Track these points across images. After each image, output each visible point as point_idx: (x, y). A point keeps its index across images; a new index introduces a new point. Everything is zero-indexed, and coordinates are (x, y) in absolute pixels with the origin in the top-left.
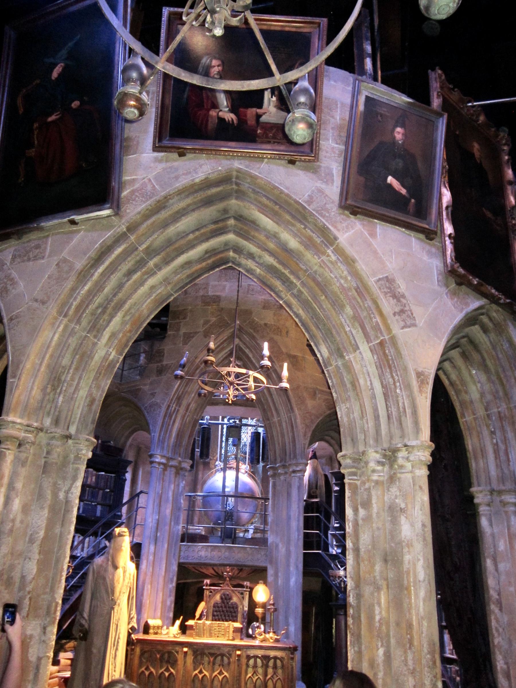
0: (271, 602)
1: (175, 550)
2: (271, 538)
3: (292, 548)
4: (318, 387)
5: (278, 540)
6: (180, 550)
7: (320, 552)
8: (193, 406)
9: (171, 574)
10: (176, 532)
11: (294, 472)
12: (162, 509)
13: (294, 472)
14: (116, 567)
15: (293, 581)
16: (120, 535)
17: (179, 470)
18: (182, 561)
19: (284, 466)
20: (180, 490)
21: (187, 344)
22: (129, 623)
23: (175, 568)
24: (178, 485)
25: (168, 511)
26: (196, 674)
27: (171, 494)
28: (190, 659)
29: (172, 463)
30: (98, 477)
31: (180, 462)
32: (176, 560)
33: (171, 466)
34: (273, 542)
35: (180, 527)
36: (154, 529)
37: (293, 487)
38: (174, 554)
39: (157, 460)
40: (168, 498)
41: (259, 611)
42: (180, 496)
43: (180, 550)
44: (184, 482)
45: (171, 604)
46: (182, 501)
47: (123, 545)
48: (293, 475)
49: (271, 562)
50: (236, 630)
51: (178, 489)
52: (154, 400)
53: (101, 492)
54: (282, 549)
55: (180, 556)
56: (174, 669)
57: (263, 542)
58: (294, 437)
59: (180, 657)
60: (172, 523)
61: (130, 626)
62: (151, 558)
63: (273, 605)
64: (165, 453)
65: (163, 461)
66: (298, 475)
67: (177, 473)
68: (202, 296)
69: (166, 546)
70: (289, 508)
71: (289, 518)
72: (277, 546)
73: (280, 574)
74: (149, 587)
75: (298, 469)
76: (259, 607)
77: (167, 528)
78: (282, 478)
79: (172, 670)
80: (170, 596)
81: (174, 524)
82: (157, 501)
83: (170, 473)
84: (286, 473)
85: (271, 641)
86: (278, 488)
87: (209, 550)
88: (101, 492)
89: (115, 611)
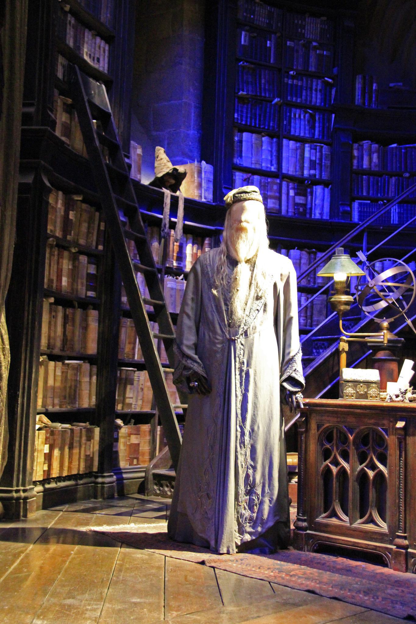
14: (234, 263)
16: (237, 200)
47: (243, 218)
53: (393, 180)
56: (385, 465)
59: (391, 440)
79: (381, 467)
88: (393, 180)
89: (238, 346)
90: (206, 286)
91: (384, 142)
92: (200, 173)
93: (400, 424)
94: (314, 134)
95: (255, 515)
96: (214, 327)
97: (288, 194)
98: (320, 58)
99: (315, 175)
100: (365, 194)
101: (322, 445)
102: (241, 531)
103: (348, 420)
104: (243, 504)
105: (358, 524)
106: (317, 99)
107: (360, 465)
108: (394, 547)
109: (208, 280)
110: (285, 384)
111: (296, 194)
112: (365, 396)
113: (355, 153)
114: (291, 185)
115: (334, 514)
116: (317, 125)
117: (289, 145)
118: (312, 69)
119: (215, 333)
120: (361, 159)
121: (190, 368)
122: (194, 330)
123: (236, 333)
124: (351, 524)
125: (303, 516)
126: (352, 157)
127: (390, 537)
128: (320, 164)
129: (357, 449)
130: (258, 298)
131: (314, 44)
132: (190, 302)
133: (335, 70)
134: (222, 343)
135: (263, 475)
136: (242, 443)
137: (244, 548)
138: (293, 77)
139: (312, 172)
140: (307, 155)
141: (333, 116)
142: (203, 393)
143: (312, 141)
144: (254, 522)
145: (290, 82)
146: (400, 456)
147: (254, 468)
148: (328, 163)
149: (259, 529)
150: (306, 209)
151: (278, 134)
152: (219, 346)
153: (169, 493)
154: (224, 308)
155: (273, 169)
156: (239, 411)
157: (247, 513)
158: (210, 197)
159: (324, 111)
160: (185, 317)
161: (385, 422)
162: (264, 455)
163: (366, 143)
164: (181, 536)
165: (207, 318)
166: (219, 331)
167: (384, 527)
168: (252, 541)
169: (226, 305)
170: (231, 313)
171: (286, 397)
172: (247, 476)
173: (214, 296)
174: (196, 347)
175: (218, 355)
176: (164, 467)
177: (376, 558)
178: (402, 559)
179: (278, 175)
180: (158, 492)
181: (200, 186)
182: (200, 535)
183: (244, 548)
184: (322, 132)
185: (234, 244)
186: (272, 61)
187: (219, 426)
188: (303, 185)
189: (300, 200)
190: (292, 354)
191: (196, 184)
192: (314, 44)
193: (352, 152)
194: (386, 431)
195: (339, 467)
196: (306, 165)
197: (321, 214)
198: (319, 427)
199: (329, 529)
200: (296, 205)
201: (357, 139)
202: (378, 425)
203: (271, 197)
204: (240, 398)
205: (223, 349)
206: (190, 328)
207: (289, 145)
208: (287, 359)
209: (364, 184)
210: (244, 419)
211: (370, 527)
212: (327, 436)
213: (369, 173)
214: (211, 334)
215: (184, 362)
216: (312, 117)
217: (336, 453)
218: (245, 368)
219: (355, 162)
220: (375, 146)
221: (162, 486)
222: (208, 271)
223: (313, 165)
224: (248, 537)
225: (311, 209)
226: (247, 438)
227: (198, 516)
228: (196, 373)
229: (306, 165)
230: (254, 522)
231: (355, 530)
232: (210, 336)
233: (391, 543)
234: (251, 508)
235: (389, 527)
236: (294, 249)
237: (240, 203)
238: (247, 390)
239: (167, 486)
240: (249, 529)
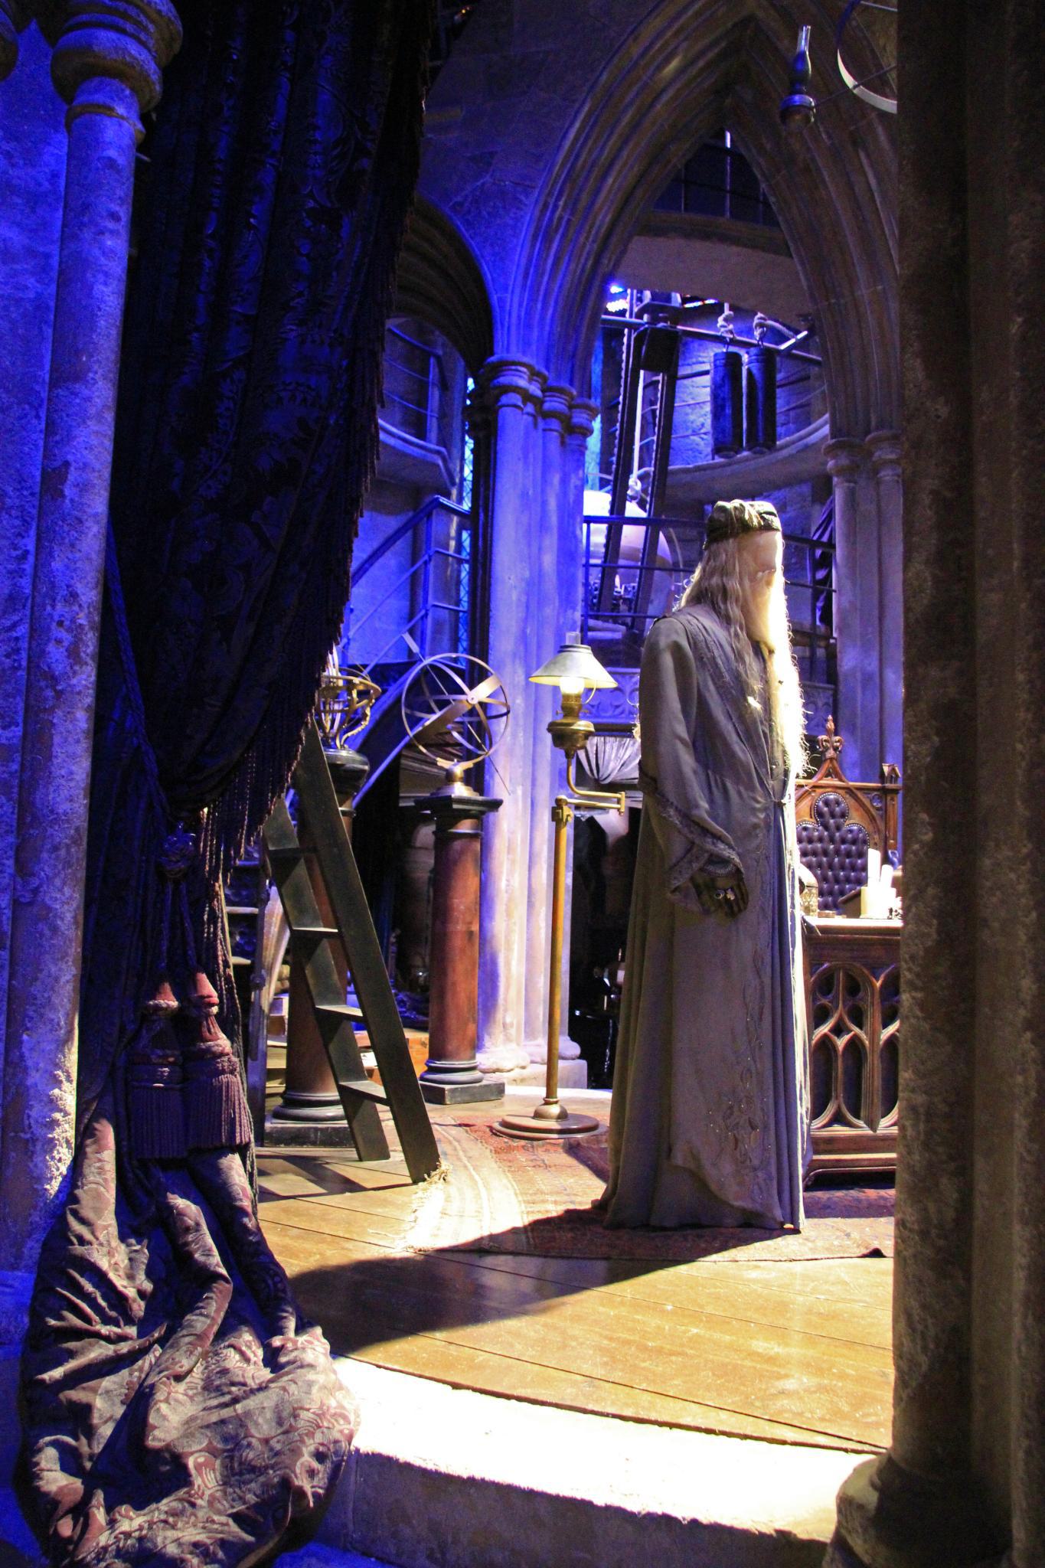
29: (554, 404)
33: (547, 415)
39: (522, 383)
65: (535, 389)
103: (873, 953)
124: (874, 1130)
134: (765, 809)
152: (762, 816)
182: (736, 1204)
199: (836, 1146)
214: (742, 789)
215: (709, 847)
222: (714, 658)
227: (728, 1167)
232: (739, 793)
237: (771, 533)
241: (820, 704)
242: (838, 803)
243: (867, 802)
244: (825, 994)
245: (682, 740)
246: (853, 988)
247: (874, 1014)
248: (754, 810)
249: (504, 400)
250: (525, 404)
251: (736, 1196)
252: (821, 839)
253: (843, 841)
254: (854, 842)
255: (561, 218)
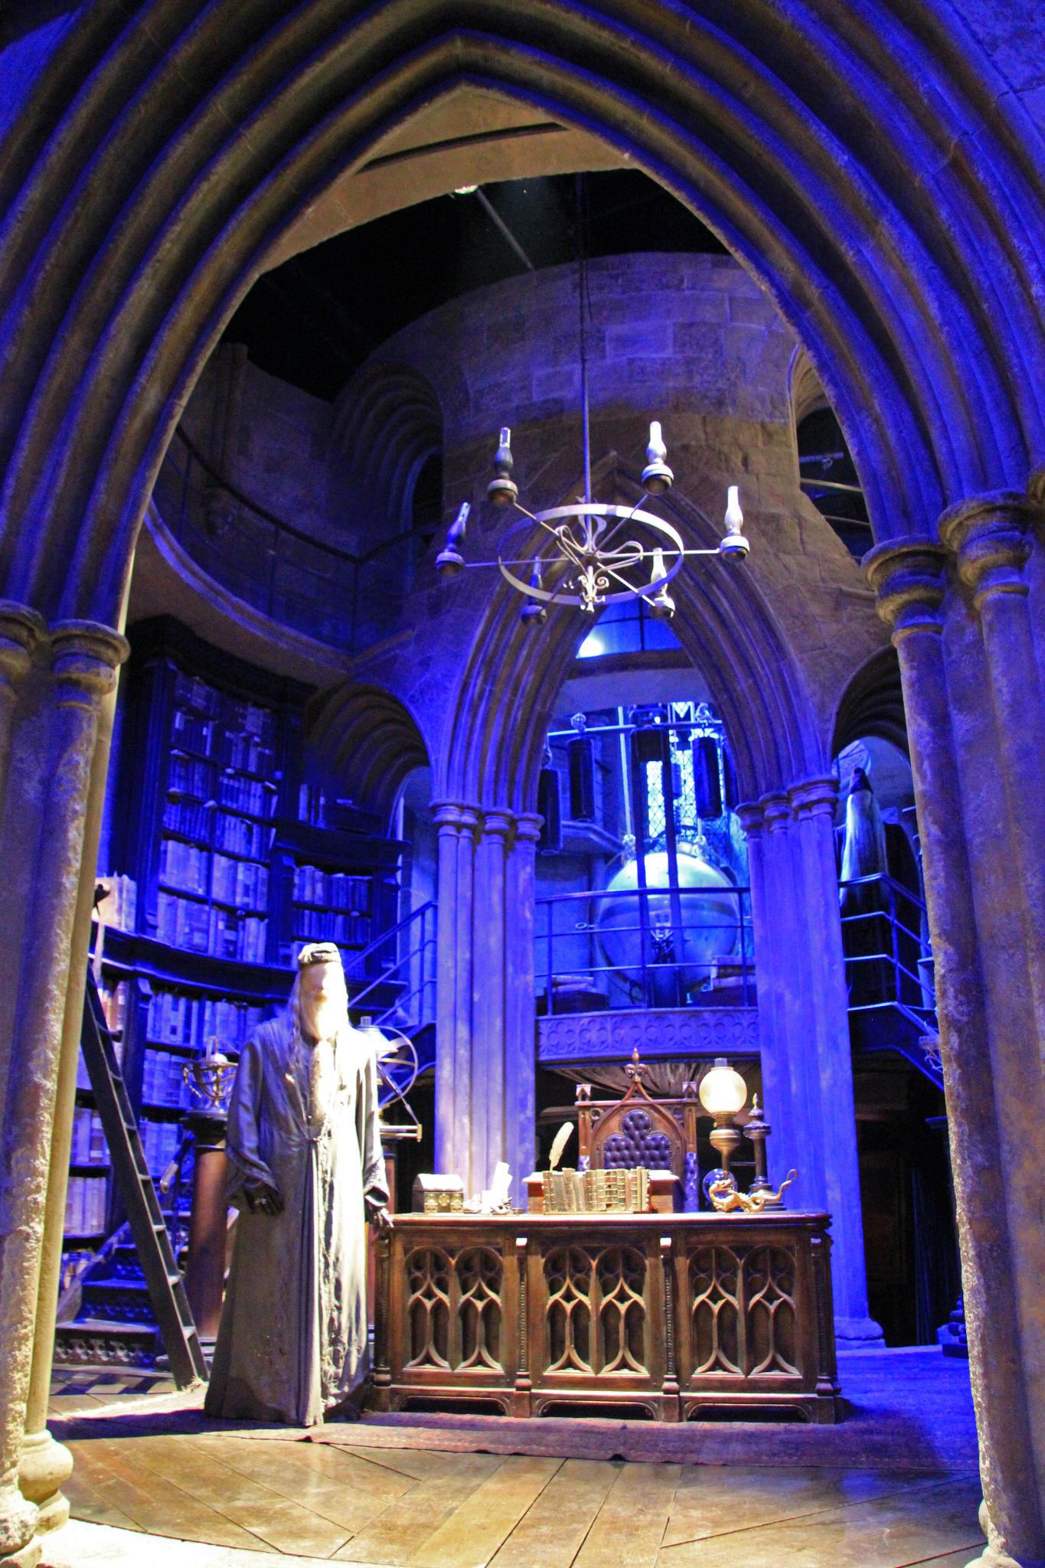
0: (755, 1111)
1: (523, 1032)
2: (762, 983)
3: (817, 999)
4: (844, 588)
5: (781, 986)
6: (538, 1034)
7: (895, 1003)
8: (529, 680)
9: (520, 1090)
10: (521, 991)
11: (806, 806)
12: (479, 934)
13: (806, 806)
14: (312, 1041)
15: (825, 1078)
16: (317, 961)
17: (510, 840)
18: (543, 1057)
19: (777, 799)
20: (521, 889)
21: (493, 528)
22: (365, 1182)
23: (528, 1075)
24: (516, 877)
25: (495, 942)
26: (556, 1303)
27: (496, 898)
28: (537, 1263)
29: (492, 824)
30: (329, 885)
31: (513, 823)
32: (527, 1056)
33: (489, 833)
34: (767, 994)
35: (530, 978)
36: (462, 985)
37: (804, 844)
38: (523, 1041)
39: (451, 817)
40: (490, 906)
41: (721, 1136)
42: (523, 903)
43: (538, 1034)
44: (528, 869)
45: (527, 1159)
46: (528, 915)
47: (325, 983)
48: (802, 815)
49: (769, 1042)
50: (656, 1188)
51: (516, 887)
52: (428, 676)
54: (793, 1005)
55: (537, 1047)
56: (497, 1292)
57: (747, 995)
58: (794, 720)
59: (509, 1262)
60: (510, 969)
61: (368, 1187)
62: (463, 1052)
63: (760, 1118)
64: (471, 800)
65: (468, 819)
66: (815, 812)
67: (508, 850)
68: (517, 408)
69: (498, 1023)
70: (799, 901)
71: (803, 925)
72: (780, 999)
73: (792, 1068)
74: (466, 1120)
75: (813, 797)
76: (720, 1127)
77: (497, 980)
78: (776, 827)
79: (493, 1295)
80: (522, 1141)
81: (516, 971)
82: (463, 917)
83: (491, 851)
84: (784, 816)
85: (755, 1207)
86: (769, 856)
87: (609, 1026)
88: (340, 919)
89: (321, 1149)
90: (271, 1069)
91: (329, 870)
92: (121, 891)
93: (521, 1242)
94: (250, 851)
95: (340, 1371)
96: (287, 1123)
97: (217, 926)
98: (261, 755)
99: (247, 905)
100: (306, 933)
101: (410, 1273)
102: (325, 1394)
104: (328, 1358)
105: (462, 1368)
106: (255, 807)
107: (464, 1293)
108: (513, 1390)
109: (275, 1062)
110: (369, 1198)
111: (228, 927)
112: (447, 1209)
113: (296, 880)
114: (222, 915)
115: (428, 1360)
116: (255, 840)
117: (221, 862)
118: (252, 769)
119: (289, 1132)
120: (302, 889)
121: (257, 1180)
122: (254, 1128)
123: (318, 1133)
125: (386, 1365)
126: (293, 885)
127: (509, 1378)
128: (255, 891)
129: (460, 1275)
130: (342, 1087)
131: (257, 739)
132: (247, 1089)
133: (279, 775)
134: (300, 1145)
135: (350, 1317)
136: (327, 1276)
137: (331, 1415)
138: (230, 776)
139: (246, 900)
140: (240, 877)
141: (274, 831)
142: (273, 1213)
143: (247, 859)
144: (340, 1381)
145: (226, 781)
146: (522, 1279)
147: (339, 1309)
148: (265, 890)
149: (346, 1389)
150: (233, 948)
151: (210, 847)
153: (84, 1357)
154: (301, 1100)
155: (201, 892)
156: (322, 1236)
157: (331, 1370)
158: (132, 924)
159: (263, 822)
160: (241, 1109)
161: (499, 1240)
162: (350, 1292)
163: (309, 869)
164: (229, 1409)
165: (278, 1113)
166: (295, 1130)
167: (498, 1368)
168: (338, 1405)
169: (304, 1096)
170: (311, 1108)
171: (370, 1212)
172: (332, 1320)
173: (287, 1084)
174: (259, 1151)
175: (294, 1162)
176: (68, 1319)
177: (490, 1407)
178: (526, 1402)
179: (205, 900)
180: (64, 1356)
181: (120, 909)
183: (331, 1415)
184: (260, 849)
185: (312, 1016)
186: (208, 753)
187: (297, 1256)
188: (235, 917)
189: (230, 935)
190: (373, 1161)
191: (116, 906)
192: (257, 739)
193: (292, 879)
194: (500, 1251)
195: (434, 1300)
196: (240, 890)
197: (255, 956)
198: (406, 1251)
200: (227, 941)
201: (300, 862)
202: (490, 1244)
203: (199, 930)
204: (323, 1218)
205: (301, 1153)
206: (249, 1124)
207: (221, 862)
208: (369, 1165)
209: (306, 920)
210: (328, 1245)
211: (480, 1370)
212: (416, 1263)
213: (311, 906)
215: (248, 1171)
216: (250, 829)
217: (429, 1282)
218: (328, 1179)
219: (296, 892)
220: (319, 874)
221: (72, 1347)
223: (247, 891)
224: (332, 1402)
225: (242, 948)
226: (331, 1270)
228: (266, 1186)
229: (240, 890)
230: (340, 1381)
231: (459, 1376)
233: (510, 1385)
234: (336, 1362)
235: (504, 1366)
236: (220, 1000)
238: (331, 1207)
239: (81, 1347)
240: (334, 1390)
241: (745, 1024)
242: (641, 1117)
243: (670, 1117)
244: (419, 1268)
245: (245, 1106)
246: (439, 1265)
247: (454, 1282)
248: (289, 1147)
249: (442, 831)
250: (459, 832)
251: (268, 1397)
252: (627, 1148)
253: (648, 1148)
254: (657, 1148)
255: (483, 691)
